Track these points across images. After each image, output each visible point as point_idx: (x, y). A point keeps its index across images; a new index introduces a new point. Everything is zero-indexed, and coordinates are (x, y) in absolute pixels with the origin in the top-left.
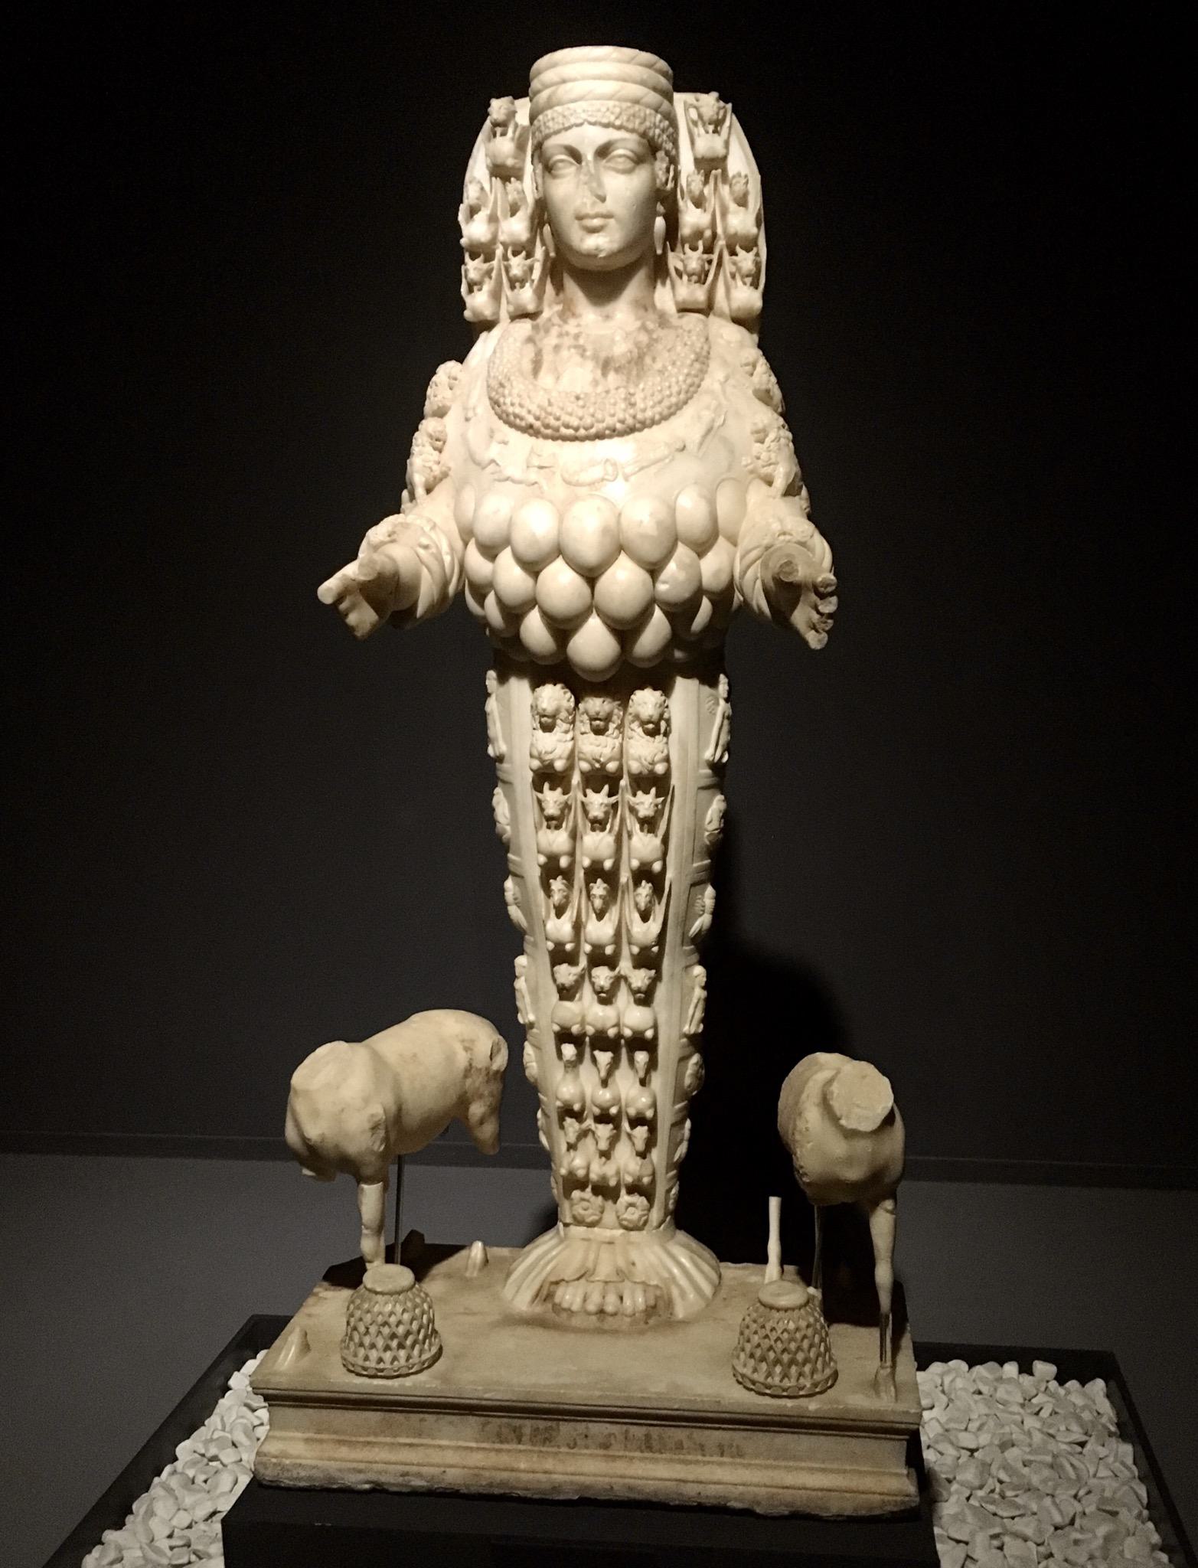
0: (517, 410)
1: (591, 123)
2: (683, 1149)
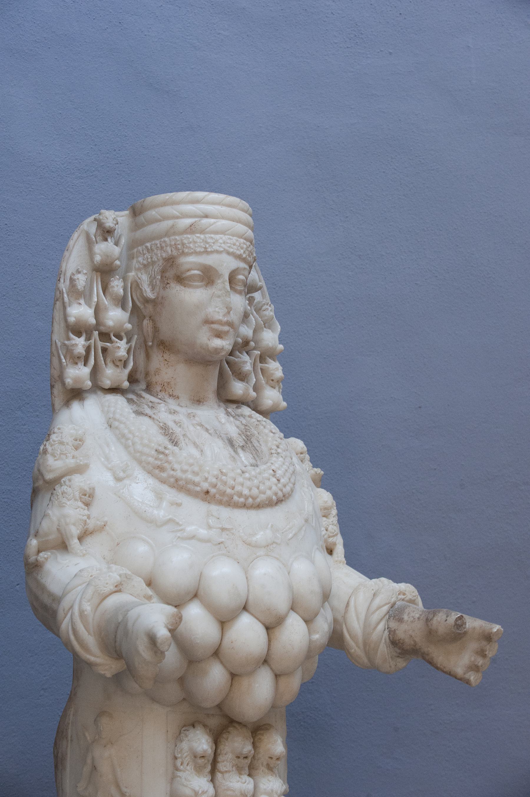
0: (190, 476)
1: (228, 253)
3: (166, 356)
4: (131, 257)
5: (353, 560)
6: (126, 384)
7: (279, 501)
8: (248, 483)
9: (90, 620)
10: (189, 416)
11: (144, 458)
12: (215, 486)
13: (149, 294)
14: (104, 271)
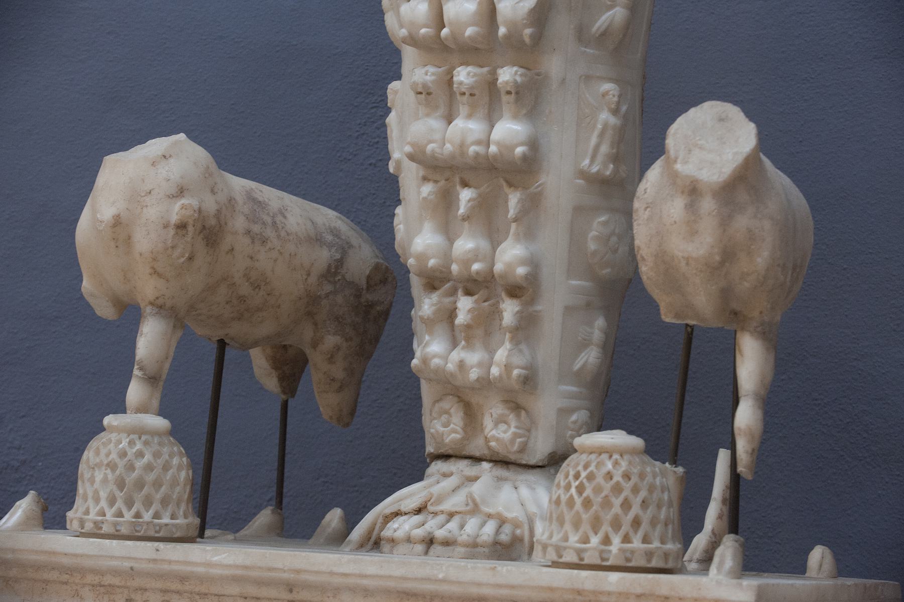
2: (591, 357)
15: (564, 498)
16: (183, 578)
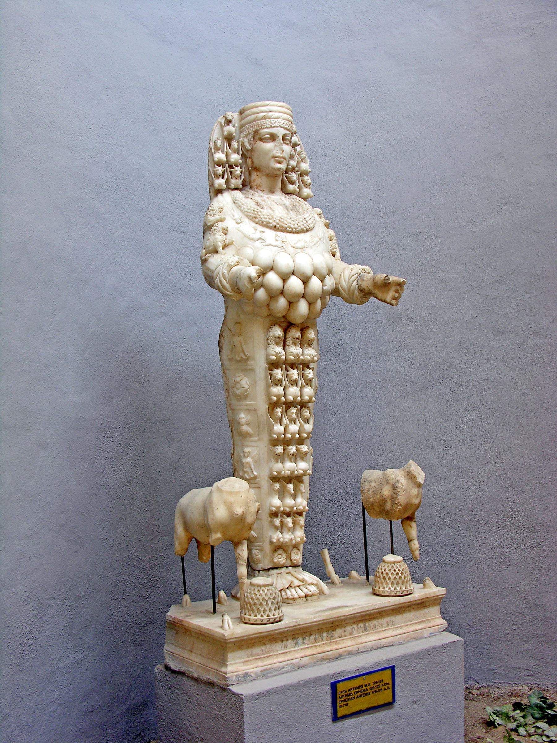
0: (268, 220)
1: (281, 127)
3: (257, 174)
4: (241, 132)
5: (343, 259)
6: (241, 186)
7: (307, 231)
8: (293, 223)
9: (227, 277)
10: (268, 198)
11: (248, 214)
12: (278, 224)
13: (249, 147)
14: (229, 139)
15: (397, 577)
16: (300, 629)
